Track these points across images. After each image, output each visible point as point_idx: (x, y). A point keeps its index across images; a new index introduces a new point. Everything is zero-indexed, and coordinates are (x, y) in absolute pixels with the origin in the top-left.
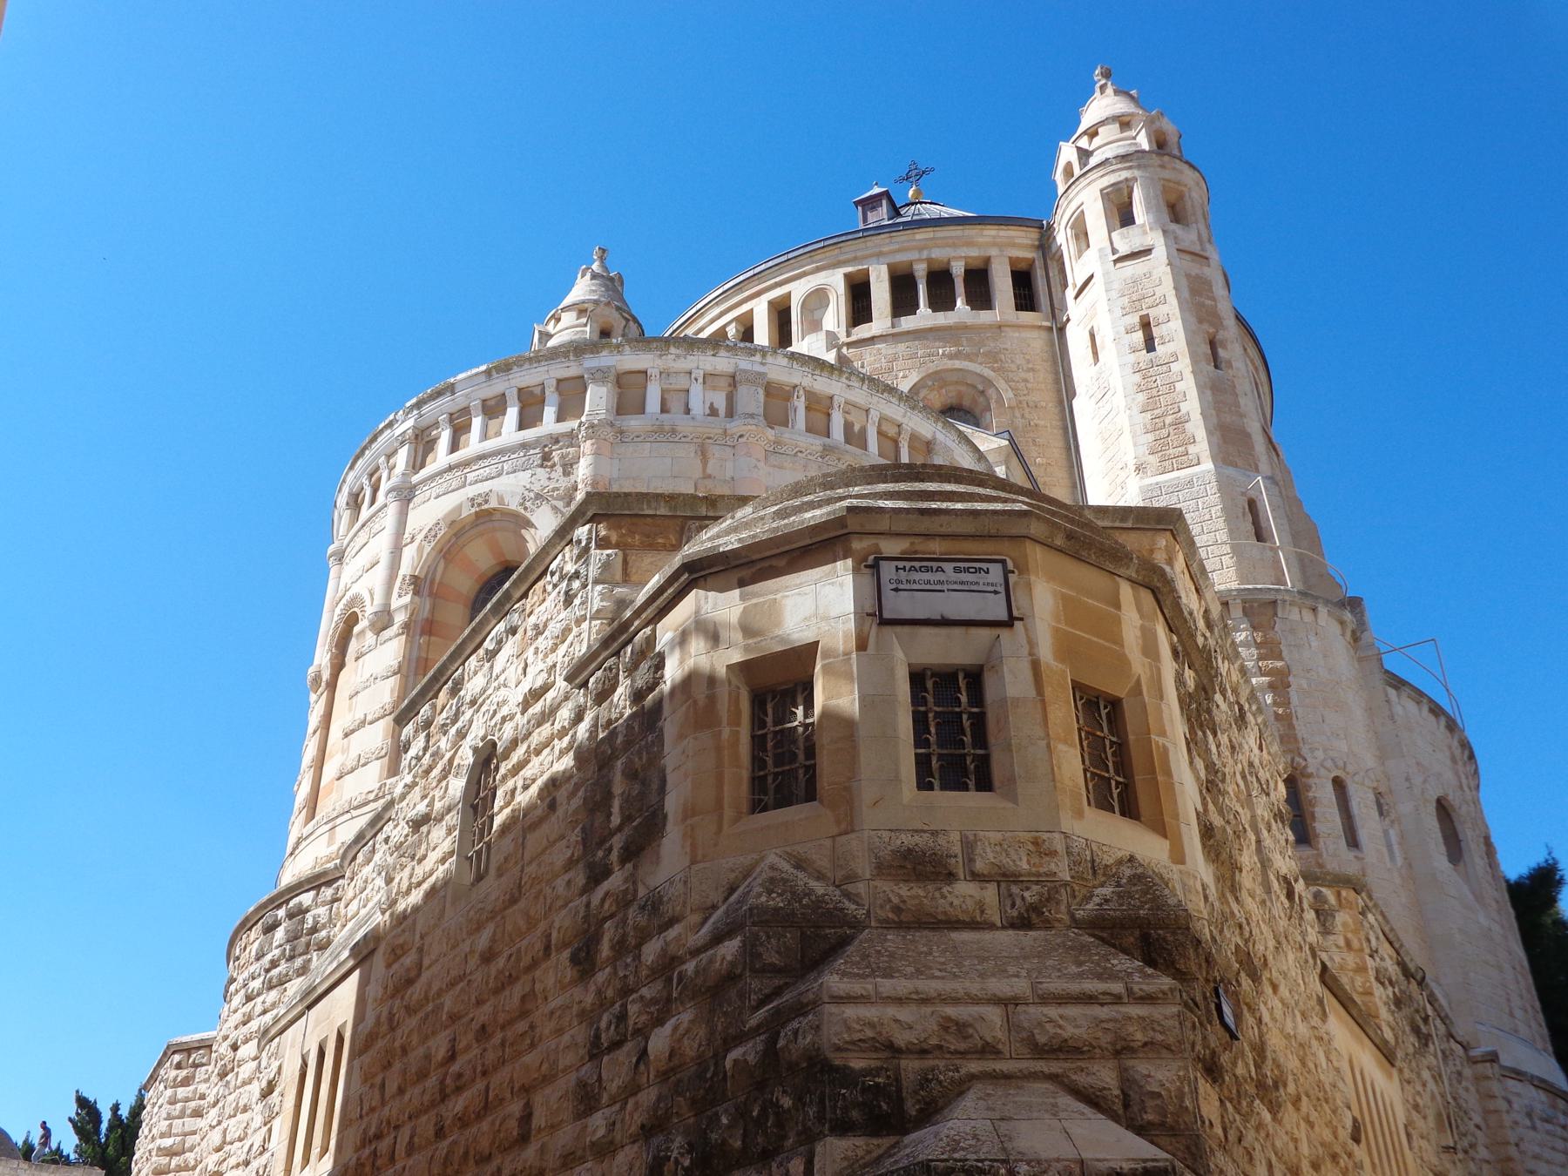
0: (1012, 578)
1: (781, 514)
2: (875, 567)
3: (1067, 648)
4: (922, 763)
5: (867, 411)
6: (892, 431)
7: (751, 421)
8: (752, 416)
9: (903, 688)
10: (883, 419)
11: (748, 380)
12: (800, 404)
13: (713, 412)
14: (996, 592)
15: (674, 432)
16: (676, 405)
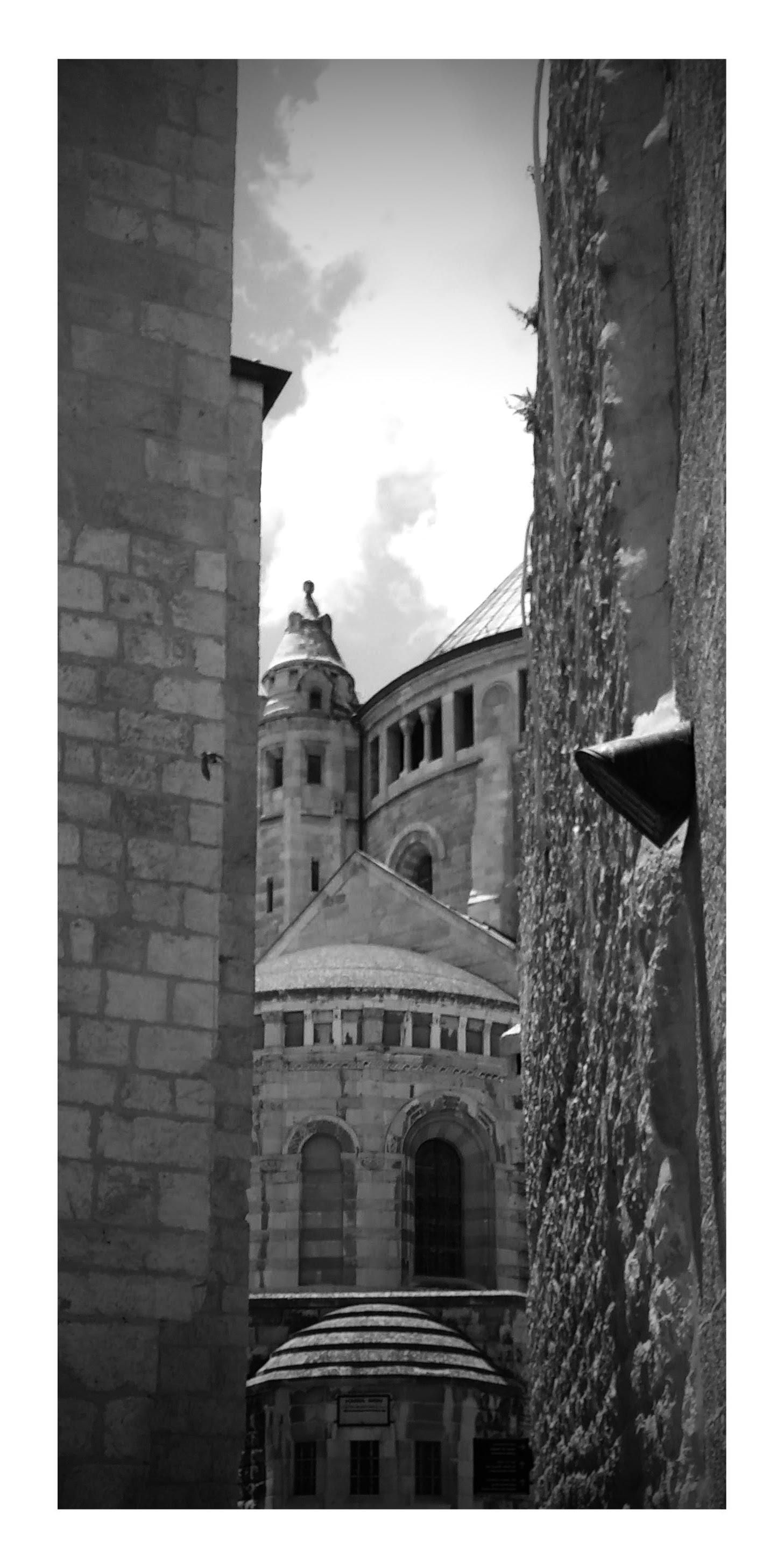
0: (392, 1403)
1: (307, 1366)
2: (338, 1400)
3: (411, 1429)
4: (353, 1482)
5: (458, 1018)
6: (476, 1027)
7: (372, 1053)
8: (371, 1048)
9: (348, 1452)
10: (469, 1019)
11: (370, 1017)
12: (408, 1025)
13: (349, 1041)
14: (384, 1411)
15: (322, 1062)
16: (323, 1036)
